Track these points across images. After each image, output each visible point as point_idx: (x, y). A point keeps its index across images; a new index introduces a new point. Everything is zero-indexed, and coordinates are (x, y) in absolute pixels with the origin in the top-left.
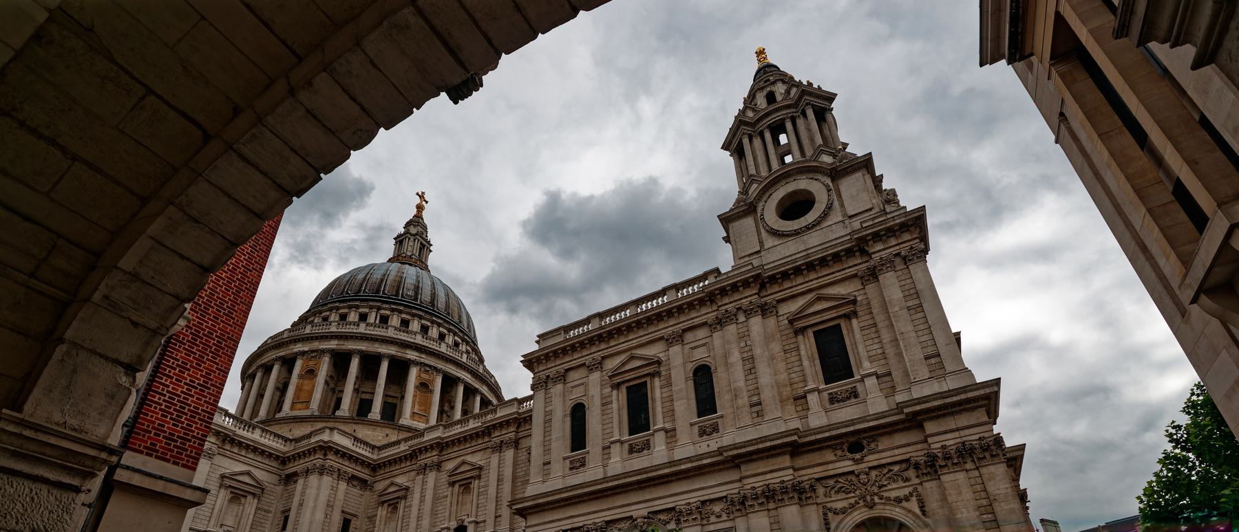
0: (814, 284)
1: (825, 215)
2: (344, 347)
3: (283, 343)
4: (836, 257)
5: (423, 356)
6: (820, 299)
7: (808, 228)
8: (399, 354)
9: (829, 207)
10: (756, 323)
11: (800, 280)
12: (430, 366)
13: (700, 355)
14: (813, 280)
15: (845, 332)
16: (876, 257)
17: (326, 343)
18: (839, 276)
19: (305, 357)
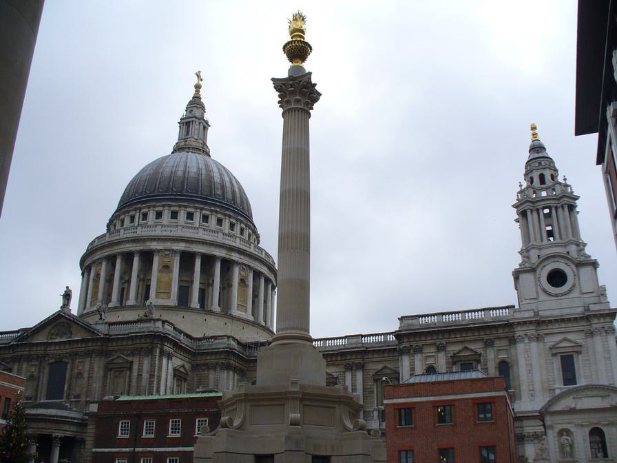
0: (563, 330)
1: (571, 290)
2: (190, 250)
3: (141, 239)
4: (576, 319)
5: (242, 257)
6: (566, 339)
7: (563, 295)
8: (228, 256)
9: (574, 286)
10: (534, 345)
11: (557, 326)
12: (246, 265)
13: (503, 356)
14: (563, 327)
15: (575, 360)
16: (594, 326)
17: (176, 244)
18: (575, 329)
19: (160, 254)
